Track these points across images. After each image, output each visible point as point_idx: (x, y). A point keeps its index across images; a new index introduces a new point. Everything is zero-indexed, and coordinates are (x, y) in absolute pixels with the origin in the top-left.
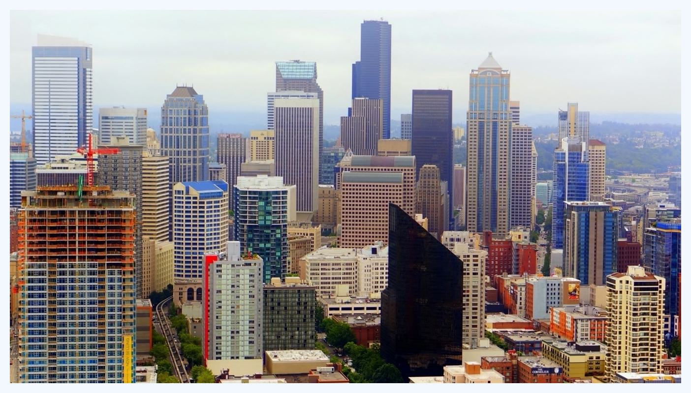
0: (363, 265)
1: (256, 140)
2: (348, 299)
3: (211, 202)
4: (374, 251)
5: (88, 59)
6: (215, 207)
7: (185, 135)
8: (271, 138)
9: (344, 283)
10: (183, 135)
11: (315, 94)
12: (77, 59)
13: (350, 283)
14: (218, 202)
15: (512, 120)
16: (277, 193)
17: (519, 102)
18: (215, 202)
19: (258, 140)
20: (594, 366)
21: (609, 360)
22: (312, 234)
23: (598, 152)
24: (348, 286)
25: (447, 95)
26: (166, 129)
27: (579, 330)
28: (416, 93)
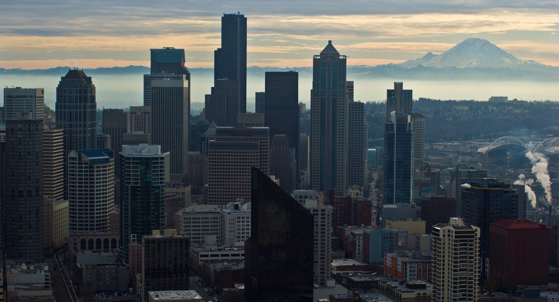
0: (228, 218)
1: (134, 115)
3: (100, 167)
4: (236, 207)
6: (103, 171)
7: (76, 110)
8: (147, 113)
9: (211, 234)
10: (75, 110)
11: (184, 76)
13: (217, 234)
18: (103, 167)
21: (434, 296)
22: (183, 193)
23: (418, 124)
24: (215, 236)
26: (61, 106)
27: (408, 271)
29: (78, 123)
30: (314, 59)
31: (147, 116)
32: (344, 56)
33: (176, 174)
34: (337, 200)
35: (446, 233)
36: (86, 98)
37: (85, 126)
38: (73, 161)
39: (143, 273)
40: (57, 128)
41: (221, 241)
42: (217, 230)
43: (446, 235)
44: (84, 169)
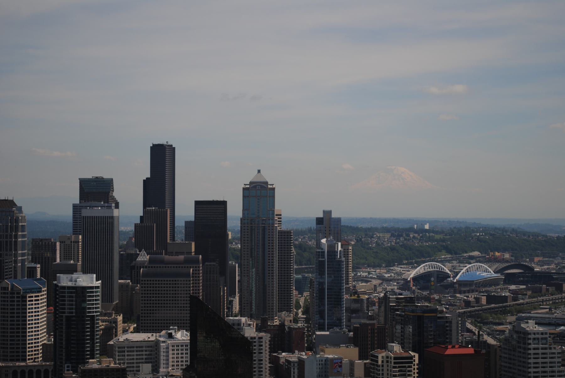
1: (63, 244)
3: (32, 297)
6: (36, 300)
7: (7, 240)
8: (76, 242)
9: (146, 363)
10: (5, 240)
11: (113, 205)
13: (151, 362)
14: (38, 296)
15: (277, 225)
16: (92, 288)
17: (281, 210)
18: (36, 296)
19: (65, 244)
24: (150, 365)
25: (223, 204)
28: (197, 203)
31: (76, 245)
35: (385, 360)
37: (16, 256)
38: (4, 291)
42: (151, 359)
43: (385, 362)
44: (16, 299)
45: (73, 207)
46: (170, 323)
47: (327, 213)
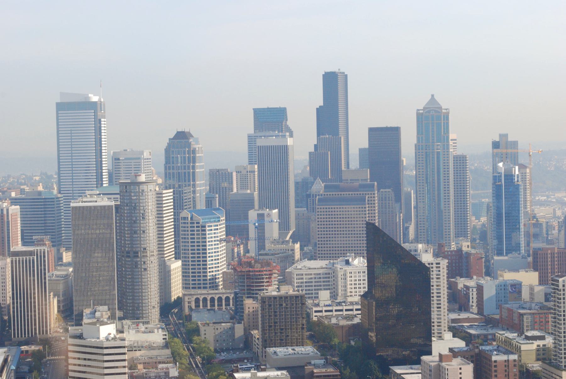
0: (340, 274)
1: (240, 174)
2: (329, 302)
3: (211, 226)
5: (103, 112)
6: (215, 230)
7: (185, 171)
9: (325, 289)
10: (183, 171)
11: (288, 134)
12: (93, 111)
13: (329, 289)
20: (541, 352)
21: (555, 347)
24: (328, 291)
25: (396, 130)
26: (169, 167)
28: (371, 130)
29: (187, 183)
30: (417, 113)
32: (446, 109)
33: (283, 232)
34: (448, 253)
36: (194, 158)
37: (194, 186)
39: (260, 329)
40: (166, 188)
41: (334, 296)
42: (329, 285)
44: (195, 229)
45: (249, 137)
46: (346, 250)
47: (504, 136)
